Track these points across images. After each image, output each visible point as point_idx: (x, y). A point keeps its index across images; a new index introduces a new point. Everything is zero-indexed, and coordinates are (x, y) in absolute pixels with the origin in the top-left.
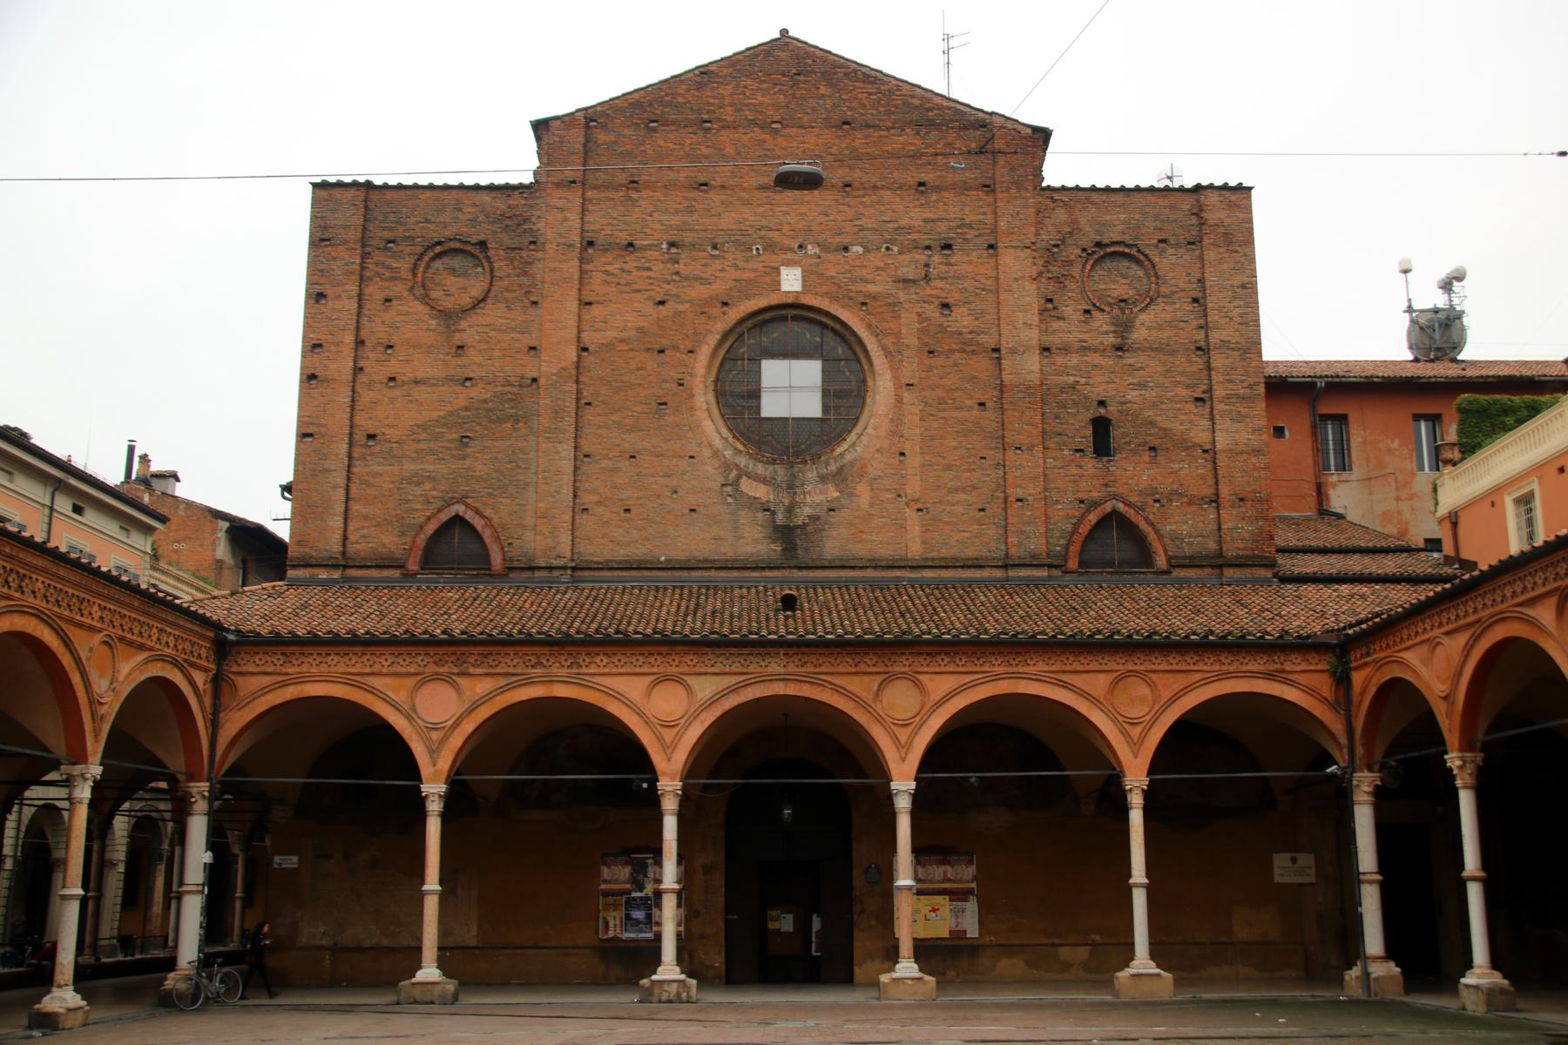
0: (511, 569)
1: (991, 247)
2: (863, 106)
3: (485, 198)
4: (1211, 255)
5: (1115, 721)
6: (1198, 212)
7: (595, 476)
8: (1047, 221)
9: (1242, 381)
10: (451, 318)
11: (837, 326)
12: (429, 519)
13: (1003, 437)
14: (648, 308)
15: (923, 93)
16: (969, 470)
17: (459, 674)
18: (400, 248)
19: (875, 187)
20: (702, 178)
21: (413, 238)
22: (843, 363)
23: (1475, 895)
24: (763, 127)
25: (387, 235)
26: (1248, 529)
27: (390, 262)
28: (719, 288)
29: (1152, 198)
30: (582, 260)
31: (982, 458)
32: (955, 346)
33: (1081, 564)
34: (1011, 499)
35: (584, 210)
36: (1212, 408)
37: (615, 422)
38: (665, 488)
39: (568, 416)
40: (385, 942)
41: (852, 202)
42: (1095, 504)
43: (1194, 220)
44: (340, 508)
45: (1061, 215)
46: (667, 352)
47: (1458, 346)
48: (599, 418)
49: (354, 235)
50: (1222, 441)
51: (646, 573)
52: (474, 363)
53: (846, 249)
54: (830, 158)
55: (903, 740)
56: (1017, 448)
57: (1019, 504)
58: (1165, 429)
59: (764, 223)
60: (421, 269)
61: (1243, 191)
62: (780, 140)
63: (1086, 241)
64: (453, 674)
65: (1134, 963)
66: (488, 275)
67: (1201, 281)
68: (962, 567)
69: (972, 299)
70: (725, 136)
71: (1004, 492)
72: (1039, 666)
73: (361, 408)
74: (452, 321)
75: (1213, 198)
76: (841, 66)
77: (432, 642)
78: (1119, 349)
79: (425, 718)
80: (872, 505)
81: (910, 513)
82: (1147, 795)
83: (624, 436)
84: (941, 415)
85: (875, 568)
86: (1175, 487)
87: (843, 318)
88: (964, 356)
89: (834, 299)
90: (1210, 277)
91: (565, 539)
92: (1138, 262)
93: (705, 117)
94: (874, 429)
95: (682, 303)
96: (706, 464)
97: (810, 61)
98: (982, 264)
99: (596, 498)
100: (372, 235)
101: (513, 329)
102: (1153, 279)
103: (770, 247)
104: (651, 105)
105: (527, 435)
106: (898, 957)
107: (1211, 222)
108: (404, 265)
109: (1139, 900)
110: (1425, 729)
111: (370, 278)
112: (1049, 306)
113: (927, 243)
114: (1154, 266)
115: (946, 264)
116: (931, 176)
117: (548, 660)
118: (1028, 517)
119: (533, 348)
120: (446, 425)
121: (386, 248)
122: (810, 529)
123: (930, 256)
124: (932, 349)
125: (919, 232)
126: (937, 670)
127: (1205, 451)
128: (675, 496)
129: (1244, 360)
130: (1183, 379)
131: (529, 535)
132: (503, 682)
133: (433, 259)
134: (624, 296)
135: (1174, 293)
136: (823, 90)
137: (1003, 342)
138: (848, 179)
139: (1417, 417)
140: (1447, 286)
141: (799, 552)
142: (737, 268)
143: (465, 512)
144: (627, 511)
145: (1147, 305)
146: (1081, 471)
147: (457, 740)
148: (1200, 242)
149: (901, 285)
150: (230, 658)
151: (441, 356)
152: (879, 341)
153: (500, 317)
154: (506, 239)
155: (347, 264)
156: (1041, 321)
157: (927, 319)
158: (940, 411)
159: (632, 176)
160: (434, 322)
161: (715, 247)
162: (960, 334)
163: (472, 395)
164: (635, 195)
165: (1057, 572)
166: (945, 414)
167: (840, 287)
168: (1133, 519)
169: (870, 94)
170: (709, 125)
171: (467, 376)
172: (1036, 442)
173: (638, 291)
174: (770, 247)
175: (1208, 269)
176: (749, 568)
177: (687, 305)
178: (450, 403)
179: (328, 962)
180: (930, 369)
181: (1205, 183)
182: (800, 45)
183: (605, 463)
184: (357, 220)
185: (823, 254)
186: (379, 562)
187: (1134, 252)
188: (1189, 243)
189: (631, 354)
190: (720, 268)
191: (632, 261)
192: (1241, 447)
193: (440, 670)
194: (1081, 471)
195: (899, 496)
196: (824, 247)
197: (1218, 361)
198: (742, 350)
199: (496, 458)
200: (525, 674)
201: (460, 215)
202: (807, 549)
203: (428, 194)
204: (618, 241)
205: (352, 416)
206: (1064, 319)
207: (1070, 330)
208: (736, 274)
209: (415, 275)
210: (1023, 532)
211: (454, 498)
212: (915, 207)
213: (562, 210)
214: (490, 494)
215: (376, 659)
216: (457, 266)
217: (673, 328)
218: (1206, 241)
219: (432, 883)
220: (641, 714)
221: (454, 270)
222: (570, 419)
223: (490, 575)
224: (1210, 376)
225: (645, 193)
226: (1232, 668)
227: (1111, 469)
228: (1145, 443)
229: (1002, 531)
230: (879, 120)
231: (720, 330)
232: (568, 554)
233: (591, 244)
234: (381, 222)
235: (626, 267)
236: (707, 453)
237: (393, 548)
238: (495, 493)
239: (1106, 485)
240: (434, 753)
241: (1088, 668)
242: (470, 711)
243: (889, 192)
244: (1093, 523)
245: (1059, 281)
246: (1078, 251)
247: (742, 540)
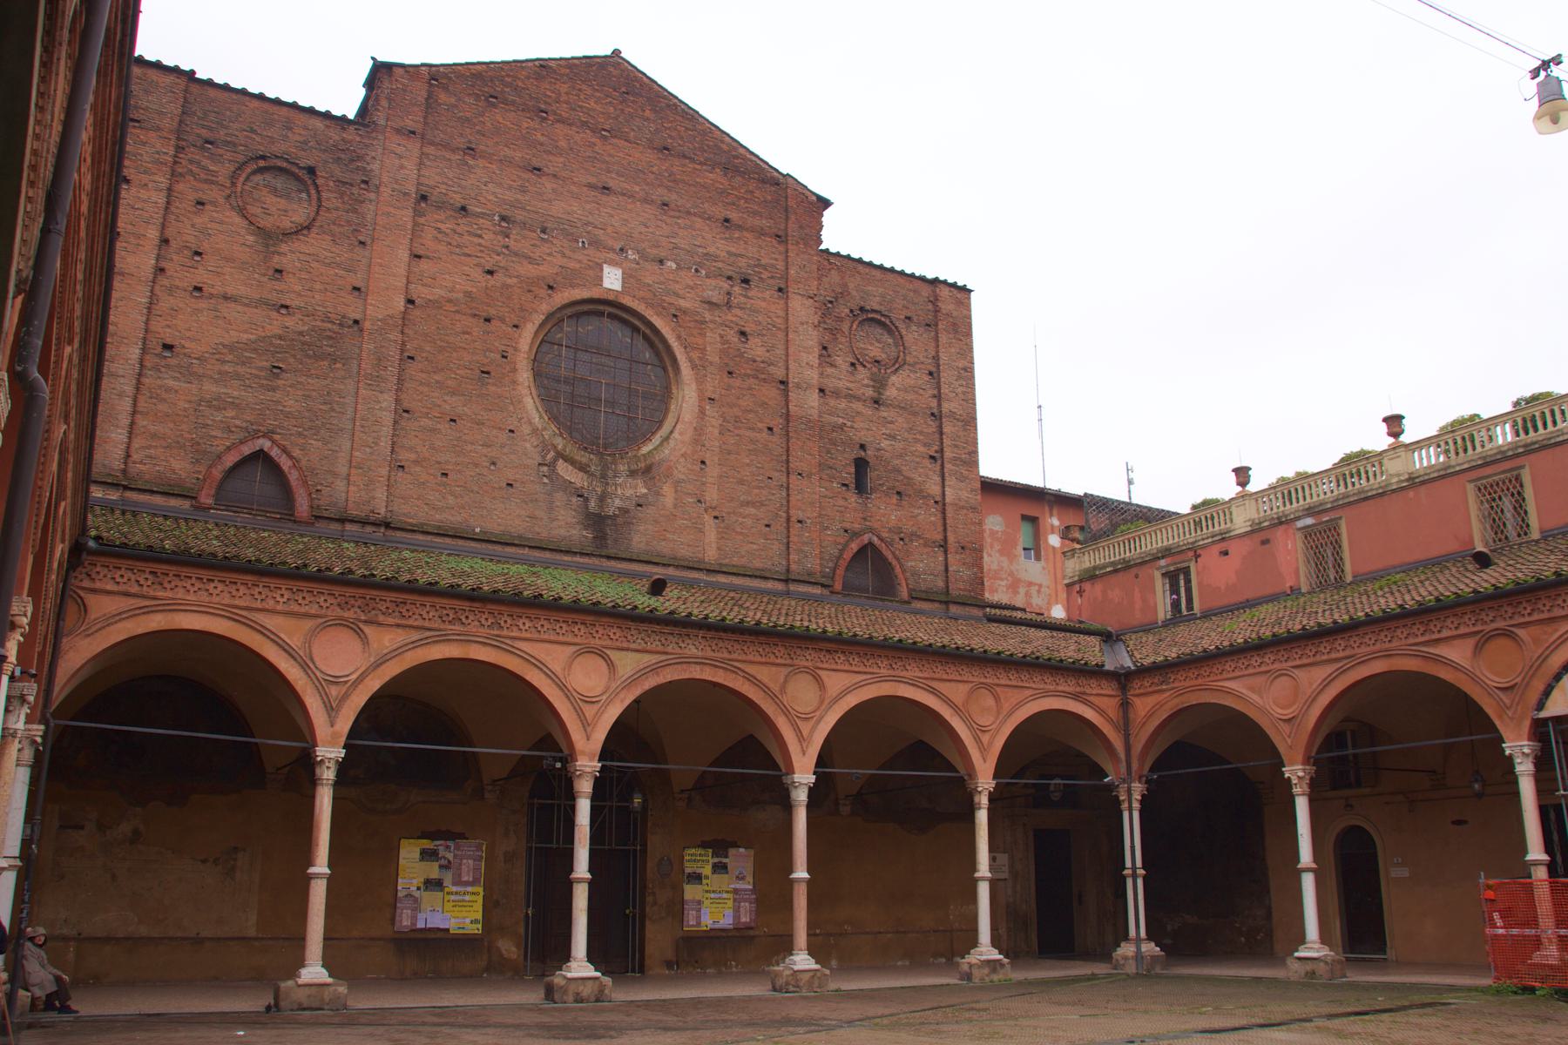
0: (318, 518)
1: (780, 290)
2: (682, 138)
3: (319, 124)
4: (943, 338)
5: (970, 728)
6: (934, 300)
7: (413, 433)
8: (824, 279)
9: (964, 448)
10: (270, 238)
11: (648, 331)
12: (229, 449)
13: (788, 462)
14: (477, 274)
15: (730, 141)
16: (759, 488)
17: (365, 622)
18: (220, 151)
19: (689, 213)
20: (536, 163)
21: (235, 145)
22: (649, 367)
23: (1308, 883)
25: (204, 132)
26: (966, 573)
27: (206, 162)
28: (547, 270)
29: (901, 280)
30: (418, 213)
31: (769, 478)
32: (749, 371)
33: (844, 588)
34: (793, 519)
36: (942, 466)
37: (437, 382)
38: (484, 458)
39: (391, 366)
40: (143, 931)
41: (668, 221)
42: (856, 535)
43: (930, 307)
45: (834, 277)
46: (493, 322)
48: (424, 375)
49: (168, 123)
51: (461, 542)
53: (661, 262)
54: (653, 176)
55: (805, 733)
56: (799, 474)
57: (800, 525)
58: (908, 478)
59: (590, 219)
60: (242, 179)
61: (966, 291)
62: (609, 147)
64: (360, 621)
65: (982, 949)
66: (314, 203)
67: (936, 358)
68: (750, 576)
69: (764, 332)
70: (560, 130)
71: (788, 512)
72: (914, 671)
73: (159, 313)
74: (271, 242)
75: (944, 292)
76: (664, 97)
77: (344, 580)
78: (876, 402)
79: (324, 668)
80: (675, 506)
81: (707, 518)
83: (446, 398)
84: (736, 432)
85: (677, 567)
86: (915, 529)
87: (657, 325)
88: (756, 382)
89: (650, 305)
90: (943, 357)
91: (381, 494)
92: (890, 332)
93: (543, 106)
94: (681, 434)
95: (510, 277)
96: (525, 440)
97: (638, 86)
98: (774, 303)
99: (413, 456)
100: (188, 129)
101: (339, 265)
102: (902, 348)
103: (595, 243)
104: (492, 81)
105: (345, 378)
106: (792, 949)
107: (944, 312)
108: (223, 171)
109: (984, 891)
111: (181, 175)
112: (824, 352)
113: (730, 273)
114: (902, 338)
115: (745, 296)
116: (734, 215)
117: (467, 617)
118: (807, 537)
119: (358, 289)
120: (255, 350)
121: (202, 148)
122: (620, 520)
123: (732, 286)
124: (731, 370)
125: (723, 262)
126: (834, 667)
127: (936, 502)
128: (492, 467)
129: (965, 430)
130: (922, 437)
131: (340, 485)
132: (415, 636)
133: (254, 173)
134: (454, 257)
135: (916, 363)
136: (648, 114)
137: (790, 376)
138: (666, 199)
141: (609, 542)
142: (564, 255)
143: (271, 447)
144: (445, 475)
145: (896, 370)
146: (845, 504)
147: (359, 699)
148: (937, 325)
149: (706, 306)
150: (80, 569)
151: (256, 276)
152: (687, 353)
153: (325, 250)
154: (338, 171)
155: (158, 153)
156: (820, 364)
157: (727, 342)
158: (735, 428)
159: (470, 142)
160: (251, 238)
161: (544, 231)
162: (755, 361)
163: (287, 324)
164: (471, 162)
165: (826, 592)
166: (741, 432)
167: (655, 295)
168: (884, 553)
169: (687, 129)
170: (545, 115)
171: (283, 303)
172: (814, 471)
173: (469, 256)
174: (595, 243)
175: (942, 350)
176: (561, 551)
177: (515, 280)
178: (263, 327)
179: (72, 955)
180: (729, 388)
181: (942, 278)
182: (630, 68)
183: (425, 422)
184: (175, 109)
185: (641, 262)
186: (166, 489)
187: (888, 322)
188: (927, 325)
189: (458, 317)
190: (548, 251)
191: (464, 225)
192: (962, 504)
193: (346, 614)
194: (845, 504)
195: (699, 501)
196: (643, 256)
197: (947, 429)
198: (559, 335)
199: (308, 396)
200: (440, 630)
201: (290, 134)
202: (616, 540)
203: (256, 103)
204: (452, 201)
205: (148, 320)
206: (832, 365)
207: (840, 378)
208: (564, 262)
209: (234, 184)
210: (802, 551)
211: (259, 431)
212: (721, 239)
213: (401, 157)
214: (300, 434)
215: (270, 594)
216: (279, 186)
217: (500, 299)
218: (940, 327)
219: (321, 866)
220: (562, 687)
221: (276, 189)
222: (393, 370)
223: (295, 522)
224: (942, 439)
225: (481, 162)
226: (1052, 688)
227: (869, 505)
228: (893, 488)
229: (784, 548)
230: (694, 154)
231: (546, 312)
232: (383, 511)
233: (424, 198)
234: (202, 119)
235: (459, 229)
236: (526, 430)
237: (184, 476)
238: (306, 433)
239: (865, 519)
241: (950, 677)
242: (377, 665)
243: (699, 220)
244: (855, 550)
245: (831, 331)
246: (847, 311)
247: (555, 523)
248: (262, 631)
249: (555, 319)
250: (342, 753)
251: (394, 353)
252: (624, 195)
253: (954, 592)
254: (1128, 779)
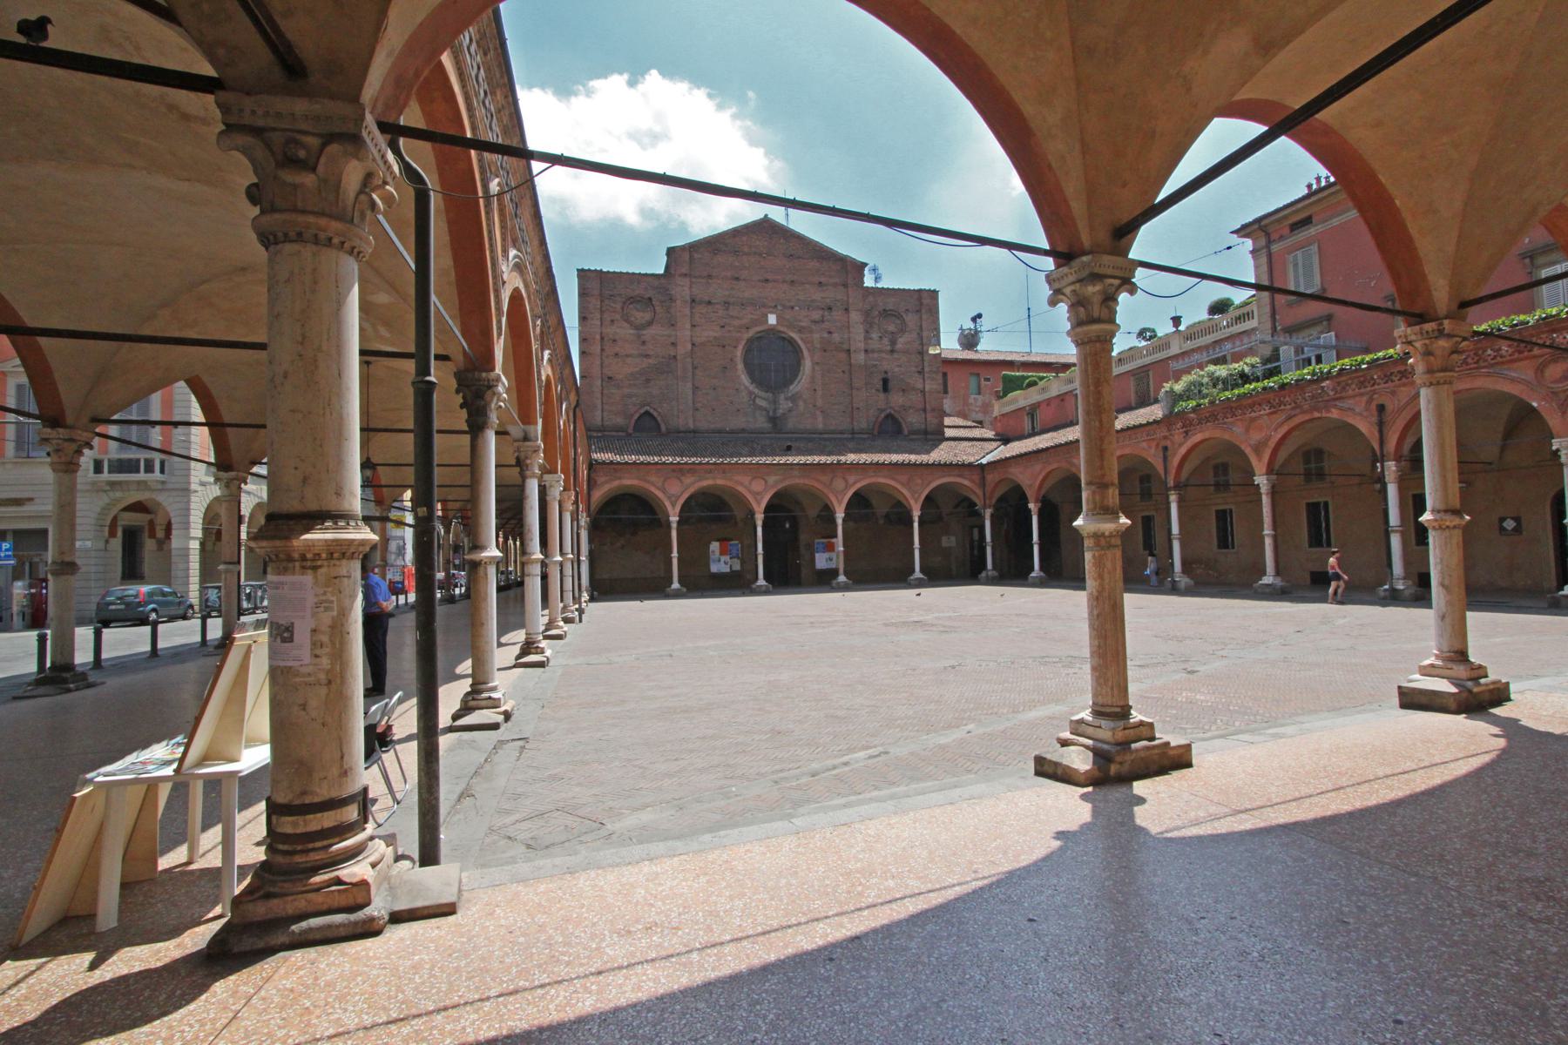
3: (650, 279)
4: (924, 317)
6: (920, 299)
14: (718, 328)
24: (760, 255)
26: (935, 421)
28: (745, 321)
30: (692, 308)
33: (879, 433)
35: (691, 287)
42: (882, 411)
44: (599, 407)
45: (871, 299)
47: (977, 344)
49: (596, 292)
50: (927, 388)
63: (881, 309)
67: (921, 326)
75: (925, 295)
81: (818, 413)
82: (920, 518)
99: (700, 405)
103: (764, 306)
108: (618, 306)
110: (1023, 498)
119: (673, 344)
136: (782, 241)
139: (971, 374)
140: (974, 319)
219: (675, 554)
222: (690, 374)
240: (673, 506)
248: (648, 482)
249: (750, 341)
250: (678, 518)
251: (690, 367)
253: (929, 429)
254: (985, 507)
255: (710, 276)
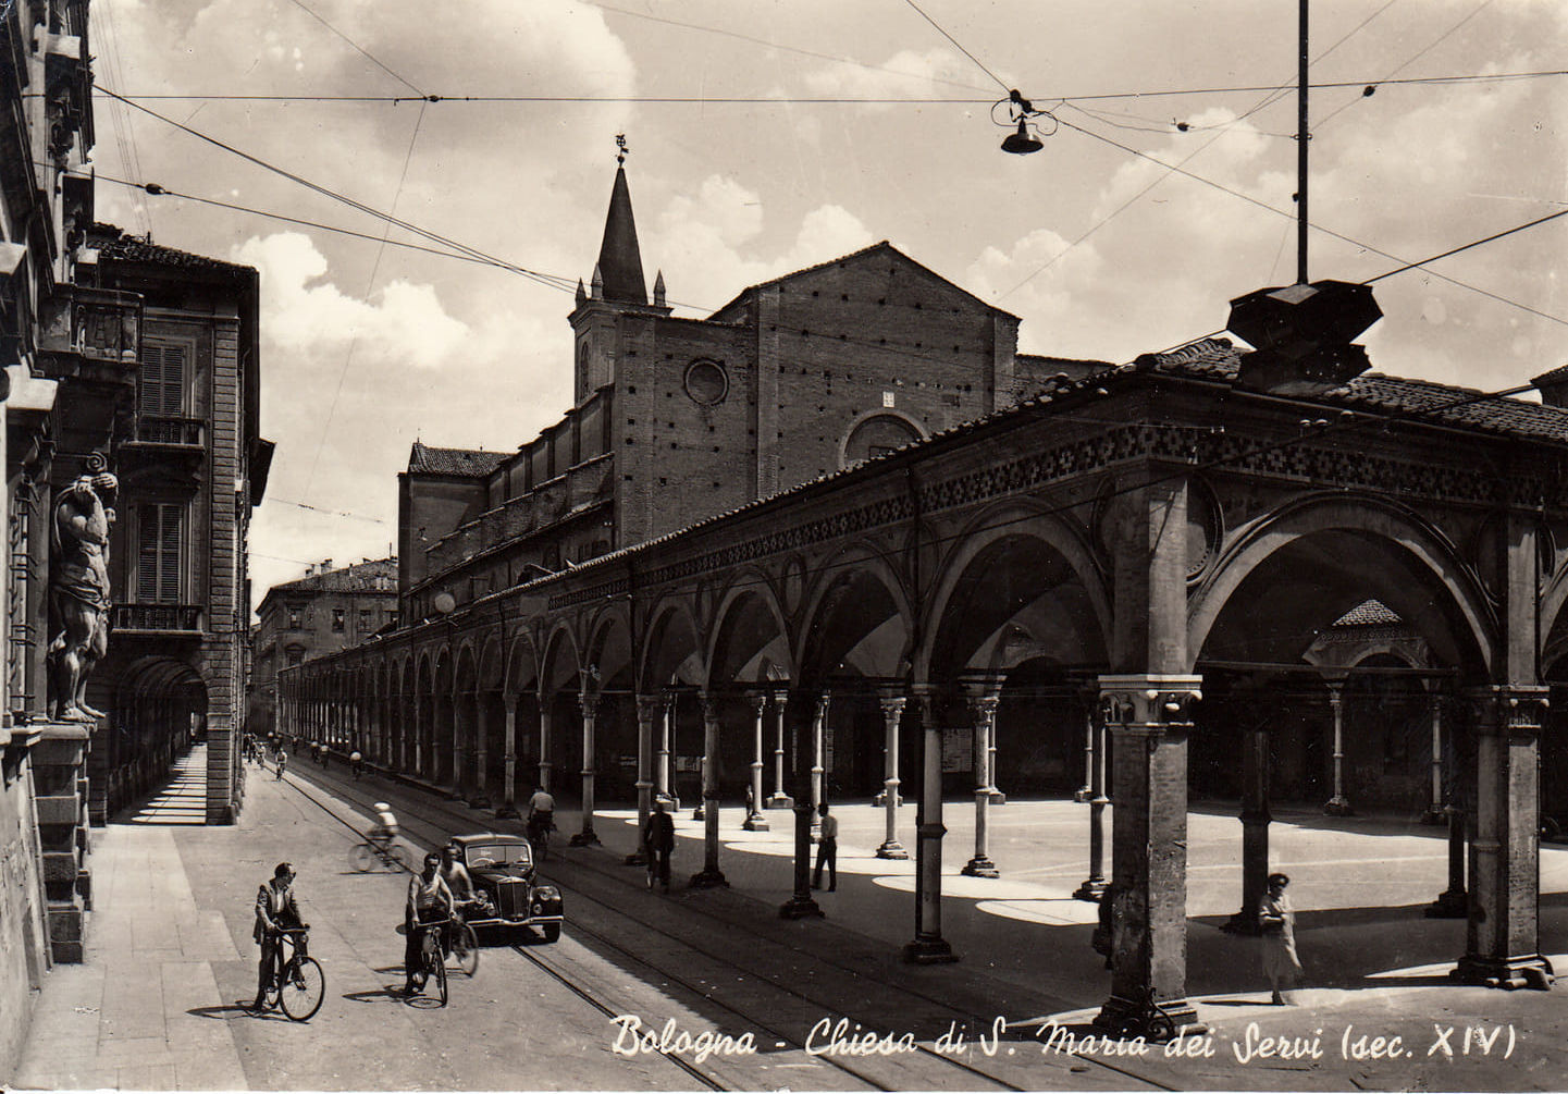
14: (814, 412)
19: (932, 347)
52: (719, 439)
53: (917, 384)
89: (911, 414)
133: (694, 369)
164: (806, 339)
252: (893, 342)
255: (805, 333)
